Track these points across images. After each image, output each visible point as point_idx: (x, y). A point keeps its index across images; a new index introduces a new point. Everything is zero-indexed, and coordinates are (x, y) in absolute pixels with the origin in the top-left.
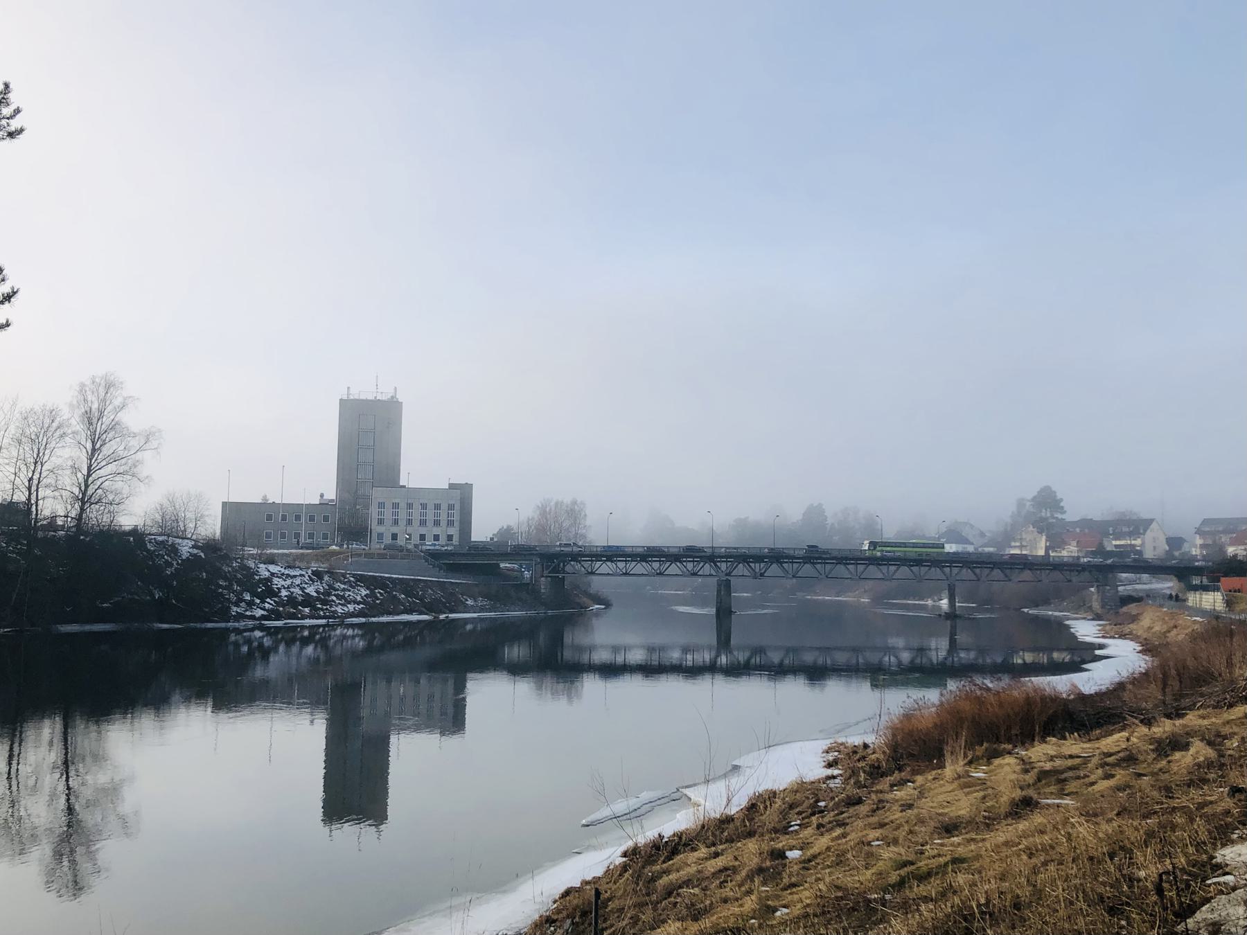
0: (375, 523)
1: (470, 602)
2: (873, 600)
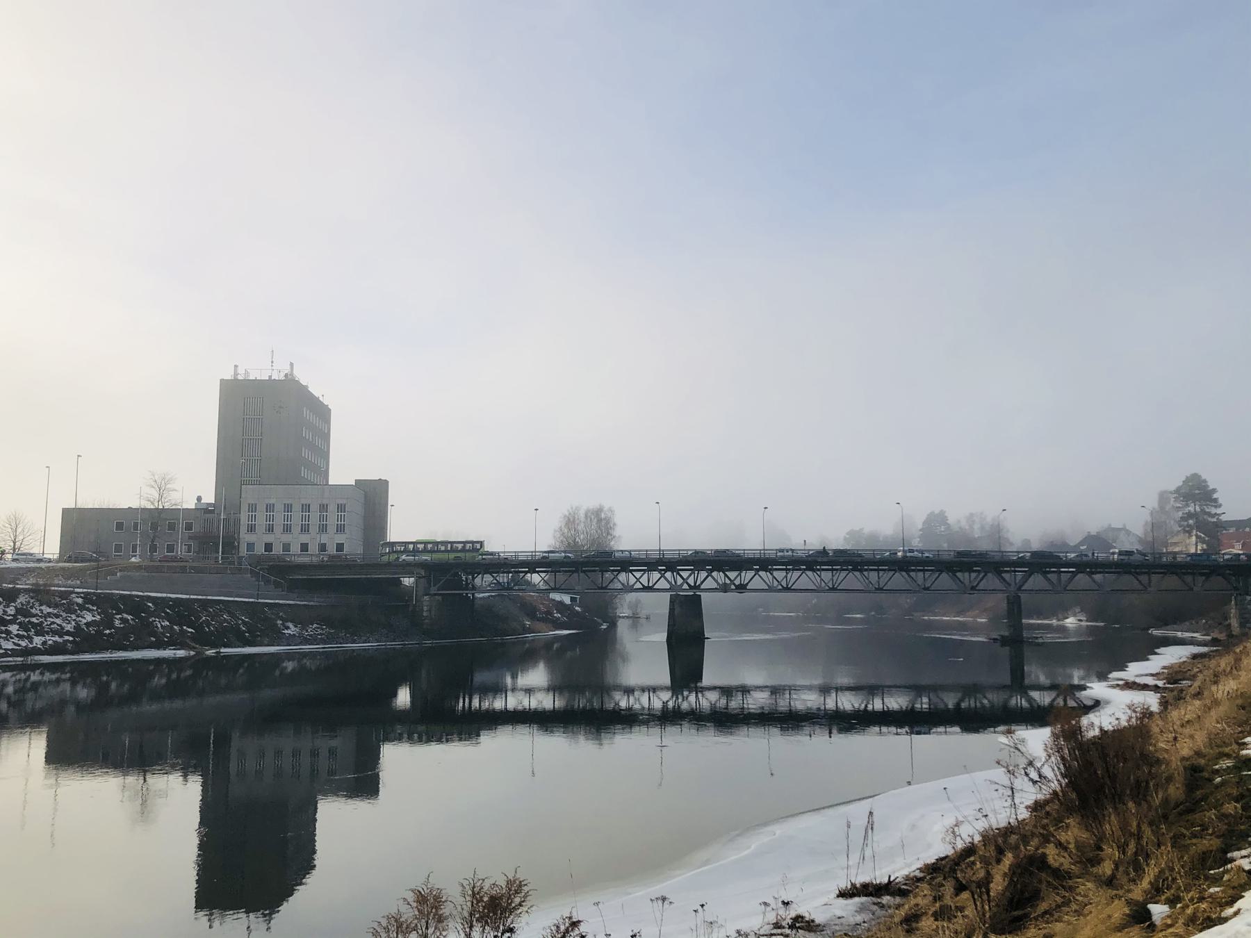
0: (243, 529)
1: (292, 630)
2: (990, 620)
